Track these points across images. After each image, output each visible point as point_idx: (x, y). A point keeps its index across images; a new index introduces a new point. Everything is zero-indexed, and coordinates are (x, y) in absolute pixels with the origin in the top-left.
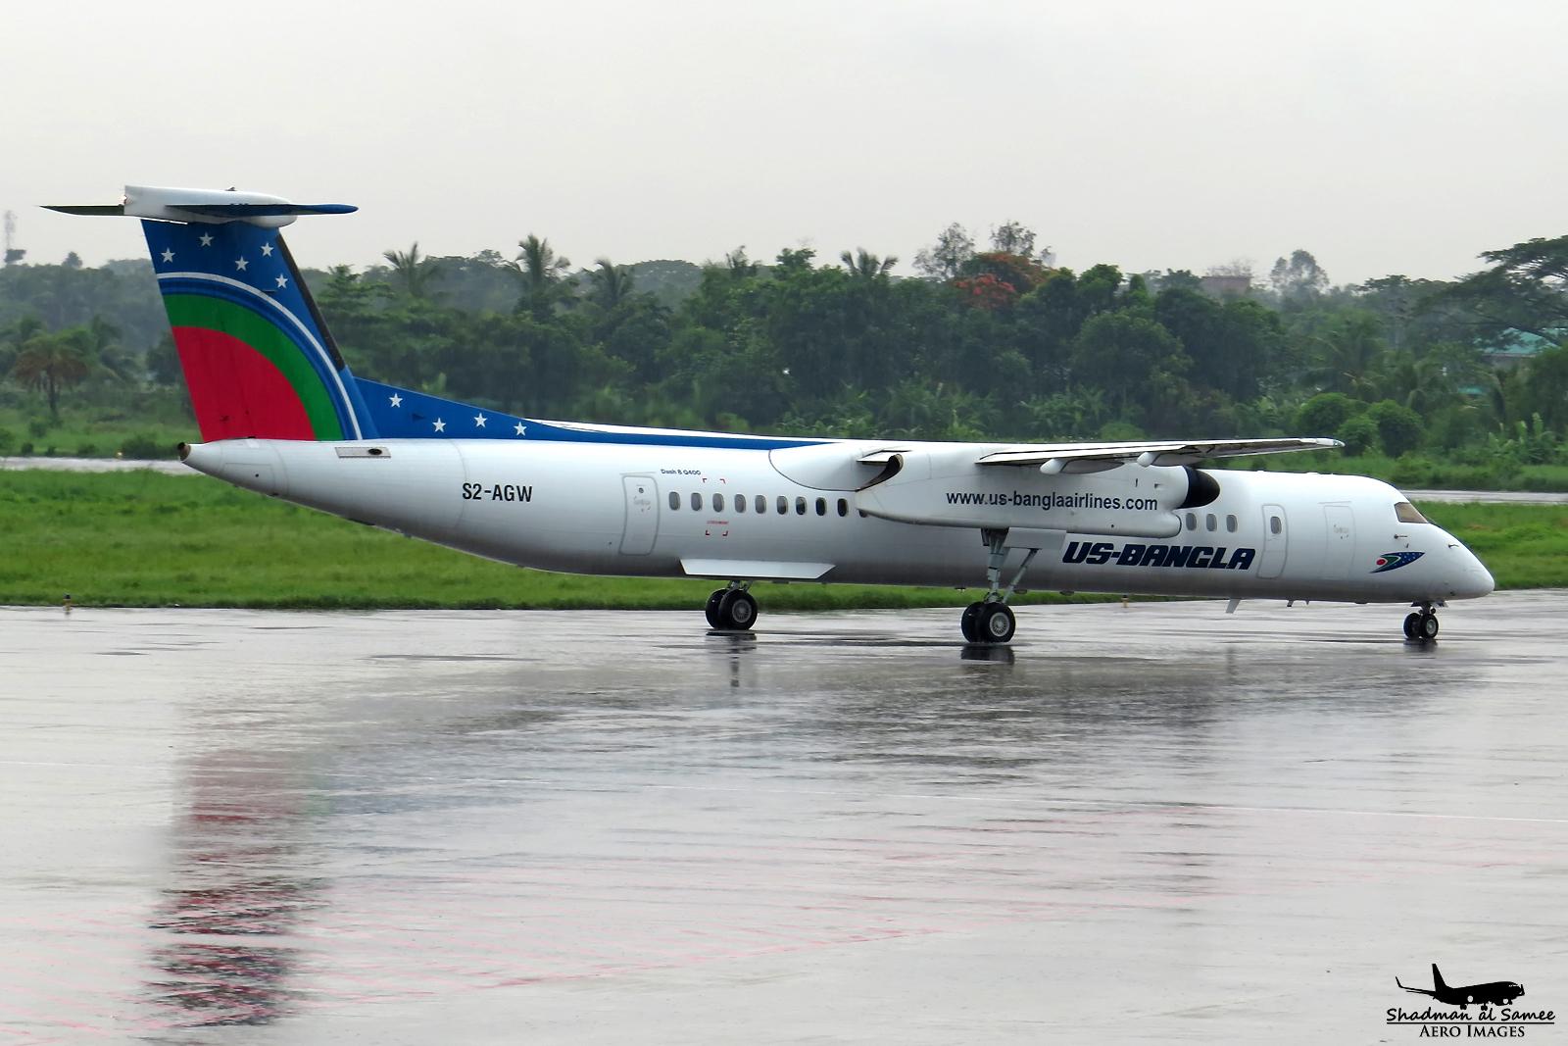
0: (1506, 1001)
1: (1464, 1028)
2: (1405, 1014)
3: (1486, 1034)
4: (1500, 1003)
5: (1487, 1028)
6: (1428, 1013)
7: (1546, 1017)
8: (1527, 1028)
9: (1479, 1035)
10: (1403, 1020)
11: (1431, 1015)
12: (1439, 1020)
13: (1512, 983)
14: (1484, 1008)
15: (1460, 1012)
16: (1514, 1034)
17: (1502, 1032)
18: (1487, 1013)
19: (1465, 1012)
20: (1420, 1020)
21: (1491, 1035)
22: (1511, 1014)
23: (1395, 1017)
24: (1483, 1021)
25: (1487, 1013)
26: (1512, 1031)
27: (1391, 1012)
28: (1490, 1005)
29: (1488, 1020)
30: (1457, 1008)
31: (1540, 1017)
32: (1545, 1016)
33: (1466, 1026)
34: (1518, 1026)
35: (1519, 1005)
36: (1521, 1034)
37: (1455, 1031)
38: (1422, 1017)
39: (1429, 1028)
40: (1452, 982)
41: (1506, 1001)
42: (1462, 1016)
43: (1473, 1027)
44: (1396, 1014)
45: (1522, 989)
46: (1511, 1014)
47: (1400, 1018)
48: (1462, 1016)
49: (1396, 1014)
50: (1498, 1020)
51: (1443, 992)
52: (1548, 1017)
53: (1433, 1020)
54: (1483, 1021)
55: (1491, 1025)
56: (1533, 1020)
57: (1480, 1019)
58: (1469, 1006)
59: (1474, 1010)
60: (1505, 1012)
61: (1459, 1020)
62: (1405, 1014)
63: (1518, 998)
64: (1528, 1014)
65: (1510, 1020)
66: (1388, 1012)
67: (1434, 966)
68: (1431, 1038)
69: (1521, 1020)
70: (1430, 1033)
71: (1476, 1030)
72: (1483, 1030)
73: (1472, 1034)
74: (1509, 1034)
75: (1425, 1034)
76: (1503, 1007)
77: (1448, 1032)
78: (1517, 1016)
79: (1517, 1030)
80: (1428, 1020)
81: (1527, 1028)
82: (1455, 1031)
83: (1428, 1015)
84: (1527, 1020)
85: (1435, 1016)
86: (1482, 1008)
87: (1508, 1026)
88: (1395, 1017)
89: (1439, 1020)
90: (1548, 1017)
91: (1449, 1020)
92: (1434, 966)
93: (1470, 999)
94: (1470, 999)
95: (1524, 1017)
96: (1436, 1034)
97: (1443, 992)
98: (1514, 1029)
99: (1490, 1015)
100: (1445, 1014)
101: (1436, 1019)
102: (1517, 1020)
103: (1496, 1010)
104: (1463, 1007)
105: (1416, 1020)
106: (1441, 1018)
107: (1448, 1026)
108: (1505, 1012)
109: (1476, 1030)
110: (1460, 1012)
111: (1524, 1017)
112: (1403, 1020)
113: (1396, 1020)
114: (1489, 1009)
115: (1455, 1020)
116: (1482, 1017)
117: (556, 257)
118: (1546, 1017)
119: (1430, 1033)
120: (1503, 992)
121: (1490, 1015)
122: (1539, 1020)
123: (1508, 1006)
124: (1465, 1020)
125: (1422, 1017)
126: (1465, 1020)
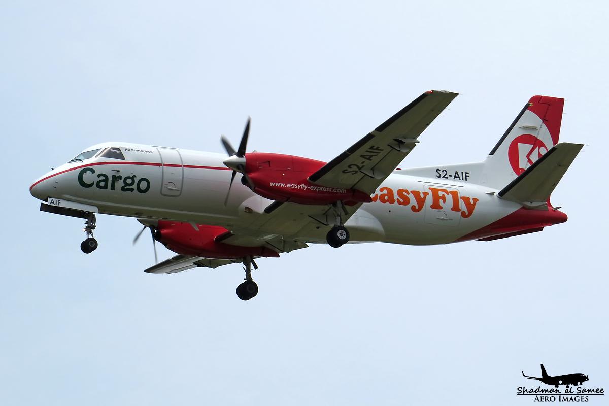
0: (579, 383)
1: (557, 397)
2: (526, 390)
3: (569, 400)
4: (576, 384)
5: (569, 397)
6: (539, 389)
7: (600, 392)
8: (590, 397)
10: (526, 393)
11: (540, 390)
12: (544, 393)
14: (568, 387)
15: (555, 389)
16: (583, 400)
17: (577, 399)
18: (569, 389)
19: (557, 389)
20: (535, 393)
21: (571, 401)
22: (581, 390)
23: (522, 391)
26: (582, 399)
27: (519, 389)
28: (570, 385)
29: (570, 393)
30: (553, 387)
31: (597, 392)
33: (558, 396)
34: (586, 396)
35: (585, 385)
36: (587, 400)
38: (535, 392)
39: (539, 397)
40: (551, 373)
41: (579, 383)
42: (556, 391)
43: (562, 397)
44: (522, 390)
45: (587, 377)
46: (581, 390)
48: (556, 391)
49: (522, 390)
50: (575, 393)
51: (546, 379)
52: (601, 392)
53: (541, 393)
54: (567, 393)
56: (593, 393)
57: (565, 392)
58: (560, 386)
59: (562, 388)
60: (579, 389)
61: (554, 393)
62: (526, 390)
63: (585, 381)
64: (591, 390)
65: (581, 393)
66: (518, 389)
67: (542, 365)
68: (540, 403)
69: (587, 393)
70: (540, 400)
71: (563, 398)
72: (567, 398)
74: (580, 400)
75: (537, 401)
76: (577, 387)
77: (549, 399)
79: (585, 398)
80: (538, 393)
81: (590, 397)
83: (539, 390)
84: (590, 393)
85: (542, 391)
86: (567, 387)
87: (580, 396)
88: (522, 391)
89: (544, 393)
90: (601, 392)
91: (549, 393)
92: (542, 365)
93: (560, 382)
94: (560, 382)
95: (588, 391)
96: (542, 400)
97: (546, 379)
98: (583, 398)
99: (571, 391)
100: (547, 390)
101: (542, 392)
102: (585, 393)
103: (574, 388)
104: (557, 386)
105: (532, 393)
106: (545, 392)
107: (548, 396)
108: (579, 389)
109: (563, 398)
110: (555, 389)
111: (588, 391)
112: (526, 393)
113: (522, 393)
114: (570, 387)
115: (553, 393)
116: (566, 391)
118: (600, 392)
119: (540, 400)
120: (577, 378)
121: (571, 391)
122: (596, 393)
123: (580, 386)
124: (558, 393)
125: (535, 392)
126: (558, 393)
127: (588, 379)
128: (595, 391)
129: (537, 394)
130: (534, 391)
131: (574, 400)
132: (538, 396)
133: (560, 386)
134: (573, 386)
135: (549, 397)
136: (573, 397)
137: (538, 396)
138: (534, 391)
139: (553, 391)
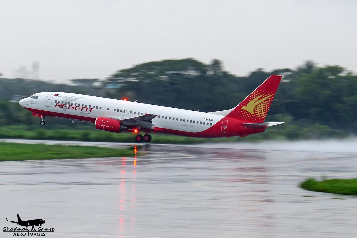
1: (27, 233)
2: (9, 229)
3: (34, 235)
4: (38, 226)
5: (34, 233)
6: (16, 229)
7: (52, 230)
8: (46, 233)
9: (31, 235)
10: (8, 231)
12: (19, 231)
13: (41, 220)
14: (33, 227)
16: (42, 235)
17: (38, 234)
18: (34, 228)
19: (27, 228)
20: (14, 231)
21: (35, 235)
22: (41, 229)
23: (6, 230)
24: (33, 231)
25: (34, 228)
26: (41, 234)
27: (5, 228)
28: (34, 226)
29: (34, 231)
30: (25, 227)
31: (50, 230)
32: (52, 229)
33: (27, 233)
34: (43, 233)
35: (43, 226)
36: (44, 235)
37: (24, 234)
39: (16, 233)
40: (23, 219)
41: (39, 225)
42: (26, 230)
43: (29, 233)
44: (6, 229)
45: (44, 221)
46: (41, 229)
47: (7, 230)
48: (26, 230)
49: (6, 229)
50: (37, 231)
51: (20, 222)
52: (52, 230)
53: (17, 231)
54: (33, 231)
55: (35, 232)
56: (48, 231)
58: (28, 226)
59: (30, 228)
60: (39, 228)
61: (25, 231)
62: (9, 229)
63: (43, 224)
64: (46, 229)
65: (41, 231)
66: (4, 228)
67: (18, 214)
69: (44, 231)
70: (17, 235)
71: (30, 234)
72: (33, 234)
73: (29, 235)
74: (40, 235)
75: (15, 235)
76: (38, 227)
77: (22, 234)
78: (43, 230)
80: (16, 231)
81: (46, 233)
82: (24, 234)
83: (16, 229)
84: (46, 231)
86: (32, 227)
87: (40, 233)
88: (6, 230)
89: (19, 231)
90: (52, 230)
91: (22, 231)
92: (18, 214)
93: (29, 224)
94: (29, 224)
95: (45, 230)
96: (18, 235)
97: (20, 222)
99: (35, 229)
100: (21, 229)
101: (18, 230)
102: (43, 231)
103: (37, 228)
104: (27, 227)
105: (12, 231)
106: (20, 230)
109: (30, 234)
111: (45, 230)
112: (8, 231)
113: (6, 231)
114: (34, 227)
115: (24, 231)
116: (32, 230)
117: (29, 68)
118: (52, 230)
119: (17, 235)
120: (39, 222)
121: (35, 229)
122: (49, 231)
123: (40, 227)
124: (27, 231)
125: (14, 230)
126: (27, 231)
127: (45, 223)
128: (49, 229)
129: (15, 231)
130: (13, 229)
131: (36, 235)
132: (15, 232)
133: (28, 226)
134: (36, 226)
135: (22, 233)
136: (36, 233)
137: (15, 232)
138: (13, 229)
139: (24, 230)
